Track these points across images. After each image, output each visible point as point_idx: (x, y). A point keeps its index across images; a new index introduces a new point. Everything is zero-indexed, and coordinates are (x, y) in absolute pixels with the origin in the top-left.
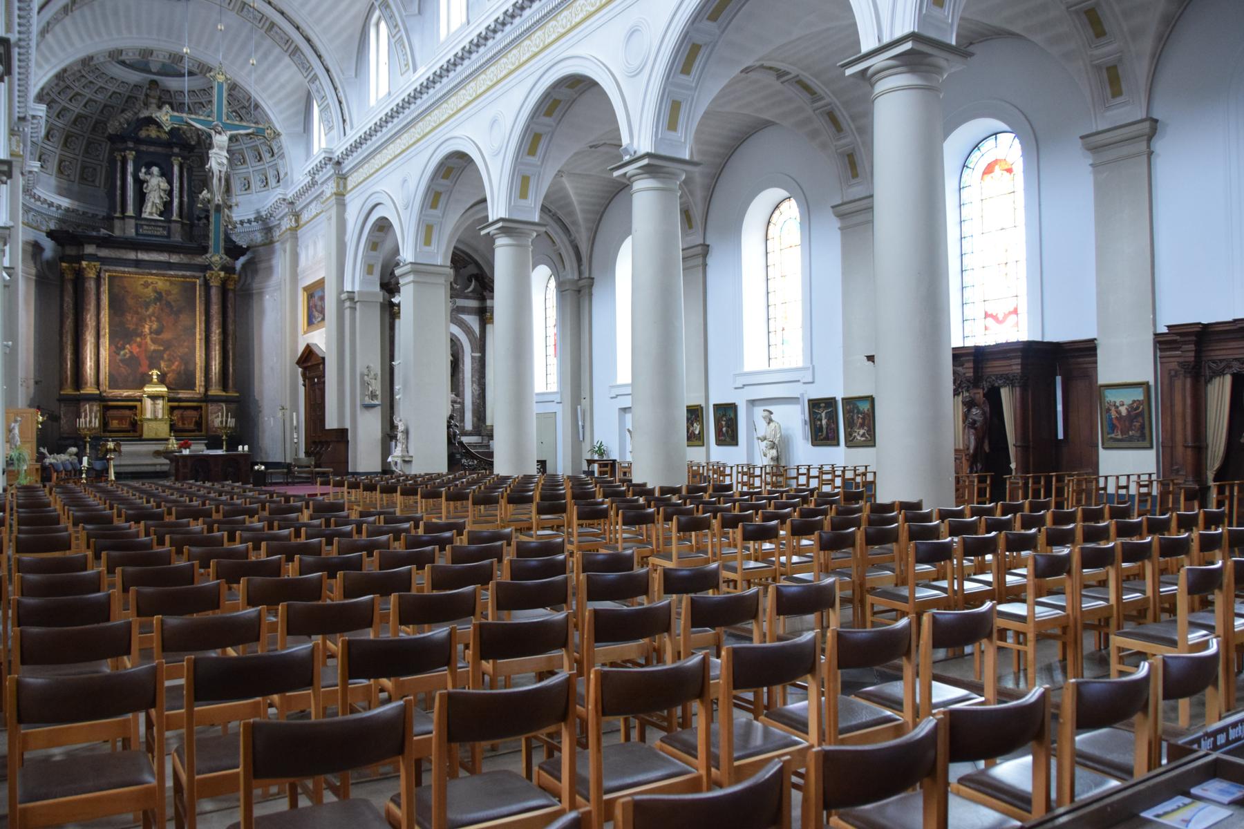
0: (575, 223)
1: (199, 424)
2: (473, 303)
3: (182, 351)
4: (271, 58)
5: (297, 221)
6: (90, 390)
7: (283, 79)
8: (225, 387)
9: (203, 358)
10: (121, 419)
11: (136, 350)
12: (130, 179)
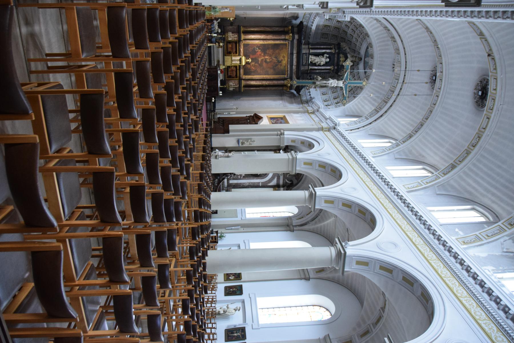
0: (316, 223)
1: (230, 77)
2: (281, 182)
3: (259, 70)
4: (373, 102)
5: (311, 113)
6: (243, 37)
7: (366, 106)
8: (245, 86)
9: (256, 78)
10: (232, 48)
11: (258, 53)
12: (324, 51)
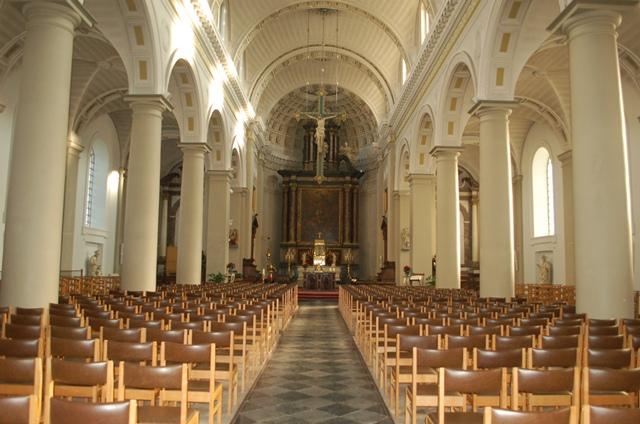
6: (292, 242)
12: (312, 145)
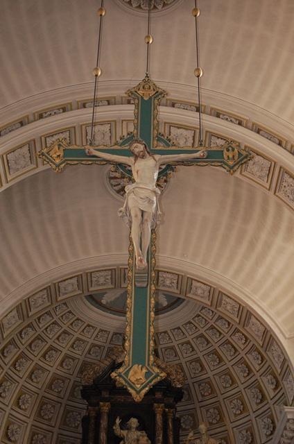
4: (259, 247)
7: (275, 272)
